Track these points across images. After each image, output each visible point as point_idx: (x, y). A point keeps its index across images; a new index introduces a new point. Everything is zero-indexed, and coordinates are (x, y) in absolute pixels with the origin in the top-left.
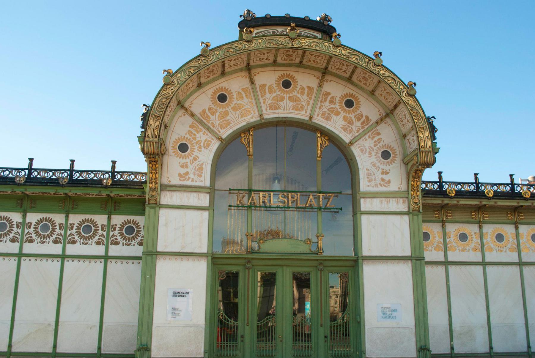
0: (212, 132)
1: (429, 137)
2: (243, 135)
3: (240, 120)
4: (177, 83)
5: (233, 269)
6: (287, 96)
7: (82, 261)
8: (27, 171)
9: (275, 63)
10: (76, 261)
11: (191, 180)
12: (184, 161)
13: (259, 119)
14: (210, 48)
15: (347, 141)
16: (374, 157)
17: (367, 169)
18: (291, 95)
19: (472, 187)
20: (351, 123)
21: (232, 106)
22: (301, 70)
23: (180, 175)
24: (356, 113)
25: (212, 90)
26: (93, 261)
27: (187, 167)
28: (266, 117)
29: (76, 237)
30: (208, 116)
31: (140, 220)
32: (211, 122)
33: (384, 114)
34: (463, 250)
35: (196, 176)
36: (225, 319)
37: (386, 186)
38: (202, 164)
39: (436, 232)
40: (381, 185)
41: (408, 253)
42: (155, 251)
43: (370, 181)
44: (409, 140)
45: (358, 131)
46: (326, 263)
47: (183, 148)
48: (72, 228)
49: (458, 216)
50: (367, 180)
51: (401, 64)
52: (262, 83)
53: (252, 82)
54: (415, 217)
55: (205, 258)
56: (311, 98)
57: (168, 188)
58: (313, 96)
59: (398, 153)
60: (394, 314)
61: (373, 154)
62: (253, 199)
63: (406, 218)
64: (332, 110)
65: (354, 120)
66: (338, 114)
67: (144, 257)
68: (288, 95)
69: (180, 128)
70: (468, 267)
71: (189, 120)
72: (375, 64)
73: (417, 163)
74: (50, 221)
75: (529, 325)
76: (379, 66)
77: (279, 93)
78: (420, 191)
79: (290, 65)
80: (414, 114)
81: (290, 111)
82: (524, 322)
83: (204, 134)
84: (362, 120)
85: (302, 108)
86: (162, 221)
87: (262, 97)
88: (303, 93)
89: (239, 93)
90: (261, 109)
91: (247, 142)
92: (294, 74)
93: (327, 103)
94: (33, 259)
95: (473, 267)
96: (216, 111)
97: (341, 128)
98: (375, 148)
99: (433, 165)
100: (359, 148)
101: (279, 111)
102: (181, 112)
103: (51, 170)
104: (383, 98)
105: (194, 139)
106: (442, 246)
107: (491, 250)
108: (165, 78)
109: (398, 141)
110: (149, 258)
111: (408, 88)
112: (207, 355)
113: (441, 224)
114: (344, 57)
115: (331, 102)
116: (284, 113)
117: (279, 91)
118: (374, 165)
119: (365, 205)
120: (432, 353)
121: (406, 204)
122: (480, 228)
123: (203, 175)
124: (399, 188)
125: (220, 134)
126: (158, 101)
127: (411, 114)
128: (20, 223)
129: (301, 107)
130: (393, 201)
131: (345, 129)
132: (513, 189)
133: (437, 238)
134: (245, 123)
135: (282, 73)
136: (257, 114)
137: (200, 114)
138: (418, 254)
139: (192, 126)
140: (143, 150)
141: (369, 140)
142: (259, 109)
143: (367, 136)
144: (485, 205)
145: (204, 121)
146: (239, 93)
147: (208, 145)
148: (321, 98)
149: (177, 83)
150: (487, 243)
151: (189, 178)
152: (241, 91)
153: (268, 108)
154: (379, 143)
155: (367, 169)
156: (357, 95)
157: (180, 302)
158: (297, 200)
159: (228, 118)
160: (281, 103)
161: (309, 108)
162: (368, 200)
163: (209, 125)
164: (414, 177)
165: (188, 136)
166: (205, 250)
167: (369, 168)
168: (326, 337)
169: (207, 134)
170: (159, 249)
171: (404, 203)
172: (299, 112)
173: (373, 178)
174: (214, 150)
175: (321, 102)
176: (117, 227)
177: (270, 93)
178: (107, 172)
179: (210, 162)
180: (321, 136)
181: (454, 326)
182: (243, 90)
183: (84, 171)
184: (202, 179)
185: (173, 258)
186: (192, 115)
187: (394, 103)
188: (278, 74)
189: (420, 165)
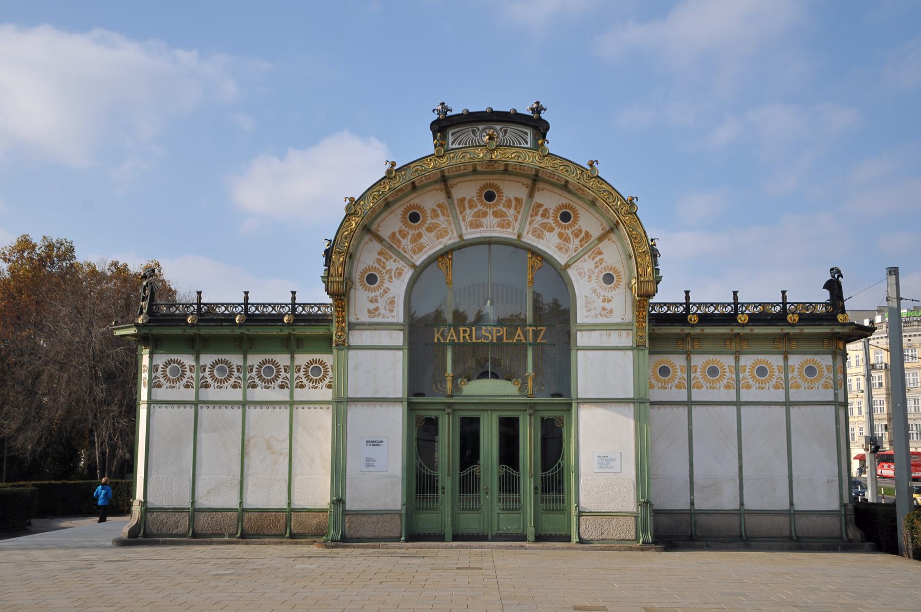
0: (404, 259)
5: (432, 414)
6: (490, 211)
7: (265, 407)
8: (195, 306)
9: (475, 171)
12: (374, 294)
14: (396, 168)
15: (563, 263)
16: (594, 281)
20: (567, 240)
21: (426, 226)
22: (507, 177)
23: (369, 311)
25: (402, 209)
27: (376, 301)
28: (466, 237)
29: (257, 381)
30: (400, 242)
33: (608, 228)
46: (538, 408)
47: (372, 279)
48: (251, 371)
49: (707, 346)
50: (585, 309)
51: (619, 177)
54: (641, 352)
55: (400, 404)
57: (357, 327)
60: (612, 463)
62: (452, 336)
63: (630, 353)
64: (544, 226)
65: (571, 236)
66: (551, 230)
69: (368, 256)
70: (717, 408)
71: (376, 246)
74: (226, 363)
75: (794, 479)
79: (494, 173)
82: (787, 474)
83: (395, 261)
84: (581, 237)
85: (509, 225)
86: (351, 364)
87: (461, 213)
88: (509, 207)
89: (434, 210)
90: (461, 228)
92: (499, 183)
93: (539, 218)
95: (723, 408)
98: (596, 271)
101: (482, 229)
102: (367, 238)
105: (384, 268)
107: (748, 387)
109: (624, 261)
112: (404, 507)
113: (685, 356)
115: (543, 216)
116: (488, 231)
118: (595, 291)
119: (582, 339)
120: (655, 507)
121: (631, 338)
123: (395, 309)
126: (340, 234)
130: (615, 334)
131: (560, 249)
133: (679, 373)
134: (441, 246)
135: (484, 182)
136: (455, 234)
138: (642, 396)
139: (380, 253)
143: (586, 257)
146: (434, 210)
147: (400, 274)
151: (380, 314)
156: (575, 205)
159: (422, 240)
160: (484, 220)
161: (518, 223)
162: (586, 333)
165: (376, 264)
166: (400, 396)
170: (349, 396)
174: (407, 280)
175: (532, 216)
179: (403, 295)
181: (695, 478)
182: (439, 206)
184: (394, 314)
185: (365, 404)
186: (380, 240)
188: (479, 184)
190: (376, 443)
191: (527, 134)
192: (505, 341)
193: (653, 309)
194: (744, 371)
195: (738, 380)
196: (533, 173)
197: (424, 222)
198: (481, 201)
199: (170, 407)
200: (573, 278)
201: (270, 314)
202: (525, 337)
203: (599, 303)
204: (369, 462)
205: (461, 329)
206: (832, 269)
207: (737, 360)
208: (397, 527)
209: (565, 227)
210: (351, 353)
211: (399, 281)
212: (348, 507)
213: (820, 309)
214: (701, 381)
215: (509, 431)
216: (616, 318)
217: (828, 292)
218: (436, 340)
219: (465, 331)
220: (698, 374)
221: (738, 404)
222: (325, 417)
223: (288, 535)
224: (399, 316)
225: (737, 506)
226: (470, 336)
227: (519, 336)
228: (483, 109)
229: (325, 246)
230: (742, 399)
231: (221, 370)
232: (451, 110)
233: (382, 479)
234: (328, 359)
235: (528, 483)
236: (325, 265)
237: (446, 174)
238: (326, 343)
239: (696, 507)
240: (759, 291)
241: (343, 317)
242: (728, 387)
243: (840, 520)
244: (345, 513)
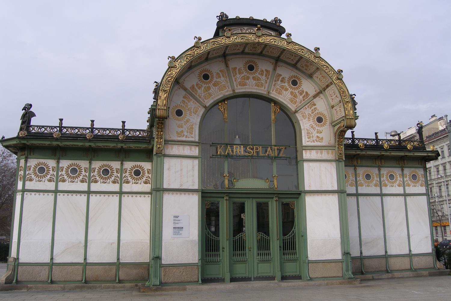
1: (352, 108)
2: (220, 104)
3: (219, 93)
4: (178, 67)
6: (251, 76)
8: (58, 128)
9: (243, 53)
10: (98, 195)
11: (185, 136)
12: (180, 122)
13: (232, 92)
14: (201, 41)
15: (294, 110)
16: (311, 121)
17: (307, 130)
18: (254, 76)
20: (295, 96)
21: (213, 82)
22: (261, 57)
23: (177, 133)
24: (299, 90)
25: (199, 71)
26: (111, 195)
27: (182, 127)
28: (237, 91)
31: (146, 166)
32: (198, 94)
33: (318, 91)
34: (368, 186)
35: (189, 133)
37: (320, 142)
41: (335, 188)
42: (162, 188)
43: (308, 138)
44: (336, 110)
45: (300, 103)
50: (307, 137)
52: (234, 66)
53: (227, 66)
54: (340, 163)
55: (197, 193)
56: (268, 78)
57: (170, 143)
58: (269, 77)
59: (328, 118)
61: (311, 119)
66: (286, 90)
67: (154, 193)
68: (252, 76)
70: (371, 197)
71: (183, 93)
72: (315, 56)
73: (344, 126)
75: (410, 236)
76: (318, 57)
78: (343, 145)
79: (253, 54)
80: (342, 92)
86: (166, 166)
87: (234, 76)
88: (262, 75)
89: (218, 74)
91: (223, 109)
92: (256, 61)
94: (66, 194)
95: (374, 197)
100: (301, 114)
103: (76, 128)
104: (318, 79)
106: (355, 183)
108: (170, 62)
110: (158, 193)
111: (337, 74)
114: (294, 50)
115: (282, 81)
117: (246, 73)
118: (312, 127)
119: (306, 155)
120: (351, 256)
122: (379, 170)
123: (194, 132)
124: (329, 143)
125: (204, 103)
127: (339, 92)
128: (55, 167)
129: (261, 84)
132: (400, 143)
133: (351, 178)
134: (222, 96)
136: (230, 89)
137: (190, 88)
138: (342, 189)
139: (184, 97)
141: (308, 109)
142: (232, 85)
144: (383, 155)
145: (194, 93)
146: (218, 74)
148: (275, 78)
149: (178, 67)
150: (384, 181)
151: (184, 135)
153: (238, 85)
154: (315, 111)
155: (307, 130)
159: (210, 91)
160: (247, 81)
161: (267, 85)
162: (308, 151)
163: (197, 96)
164: (340, 135)
165: (182, 104)
166: (196, 187)
168: (280, 247)
169: (196, 103)
170: (165, 186)
172: (260, 88)
176: (128, 170)
178: (119, 130)
180: (274, 105)
182: (220, 71)
183: (102, 129)
184: (193, 136)
185: (175, 193)
186: (185, 89)
187: (327, 84)
189: (345, 127)
197: (212, 80)
198: (246, 70)
200: (299, 119)
201: (108, 135)
203: (314, 134)
207: (379, 170)
208: (196, 274)
209: (294, 89)
214: (363, 182)
223: (117, 281)
227: (269, 152)
228: (247, 16)
229: (154, 86)
230: (383, 192)
233: (183, 244)
235: (275, 243)
241: (161, 135)
244: (162, 266)
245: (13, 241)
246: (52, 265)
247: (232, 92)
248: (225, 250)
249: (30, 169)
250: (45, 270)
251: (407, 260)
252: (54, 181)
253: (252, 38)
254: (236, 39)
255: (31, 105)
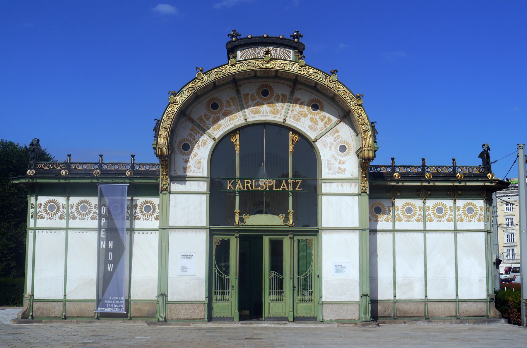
5: (226, 237)
13: (244, 121)
14: (203, 72)
16: (333, 150)
19: (420, 170)
20: (316, 122)
21: (223, 112)
24: (321, 115)
36: (220, 274)
38: (201, 159)
39: (386, 207)
40: (338, 172)
41: (356, 225)
43: (329, 170)
50: (327, 168)
53: (238, 92)
57: (176, 179)
59: (352, 147)
60: (344, 270)
61: (333, 148)
62: (239, 186)
63: (356, 198)
64: (301, 113)
65: (318, 120)
66: (305, 116)
70: (411, 234)
71: (190, 125)
74: (87, 202)
77: (259, 100)
80: (360, 120)
81: (268, 114)
82: (455, 276)
84: (325, 121)
85: (277, 112)
87: (246, 104)
89: (228, 102)
92: (271, 84)
95: (415, 234)
96: (210, 117)
97: (309, 127)
98: (335, 143)
99: (373, 159)
101: (260, 114)
107: (431, 220)
109: (353, 137)
110: (164, 231)
116: (263, 116)
118: (334, 157)
119: (325, 188)
121: (357, 187)
123: (201, 167)
126: (165, 116)
130: (346, 185)
131: (311, 128)
134: (232, 126)
135: (261, 83)
136: (242, 118)
137: (198, 119)
139: (192, 130)
140: (156, 153)
141: (330, 137)
143: (328, 134)
145: (201, 125)
146: (228, 102)
147: (205, 144)
151: (191, 170)
152: (229, 100)
157: (186, 262)
158: (273, 185)
161: (283, 111)
165: (189, 137)
167: (329, 159)
168: (294, 287)
170: (171, 224)
171: (355, 186)
173: (332, 167)
177: (252, 101)
182: (231, 99)
186: (192, 121)
190: (189, 257)
191: (290, 52)
192: (274, 189)
193: (371, 169)
194: (429, 210)
195: (424, 216)
196: (294, 78)
199: (49, 231)
202: (288, 188)
204: (184, 269)
205: (246, 181)
206: (484, 145)
208: (203, 312)
210: (172, 196)
211: (204, 148)
212: (170, 298)
213: (475, 171)
214: (402, 216)
215: (277, 249)
216: (347, 175)
217: (481, 160)
218: (228, 188)
219: (248, 183)
220: (399, 212)
221: (425, 231)
222: (154, 238)
224: (204, 171)
225: (423, 297)
226: (251, 186)
229: (154, 124)
230: (427, 229)
231: (84, 208)
232: (240, 36)
234: (156, 201)
236: (155, 137)
237: (237, 77)
238: (154, 190)
239: (397, 298)
240: (439, 159)
242: (418, 220)
243: (487, 305)
244: (167, 303)
245: (28, 278)
246: (65, 301)
247: (244, 121)
248: (234, 289)
249: (40, 207)
250: (59, 306)
251: (452, 306)
252: (64, 219)
253: (260, 64)
254: (242, 66)
255: (38, 140)
